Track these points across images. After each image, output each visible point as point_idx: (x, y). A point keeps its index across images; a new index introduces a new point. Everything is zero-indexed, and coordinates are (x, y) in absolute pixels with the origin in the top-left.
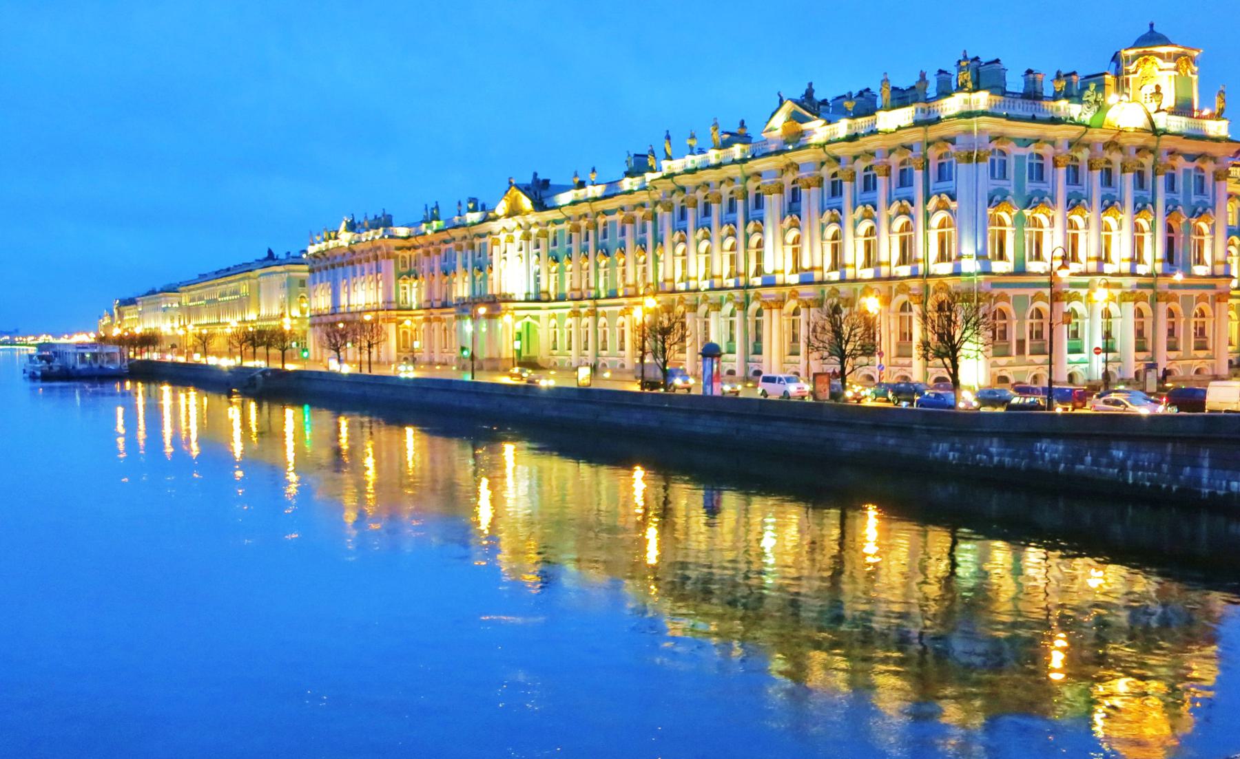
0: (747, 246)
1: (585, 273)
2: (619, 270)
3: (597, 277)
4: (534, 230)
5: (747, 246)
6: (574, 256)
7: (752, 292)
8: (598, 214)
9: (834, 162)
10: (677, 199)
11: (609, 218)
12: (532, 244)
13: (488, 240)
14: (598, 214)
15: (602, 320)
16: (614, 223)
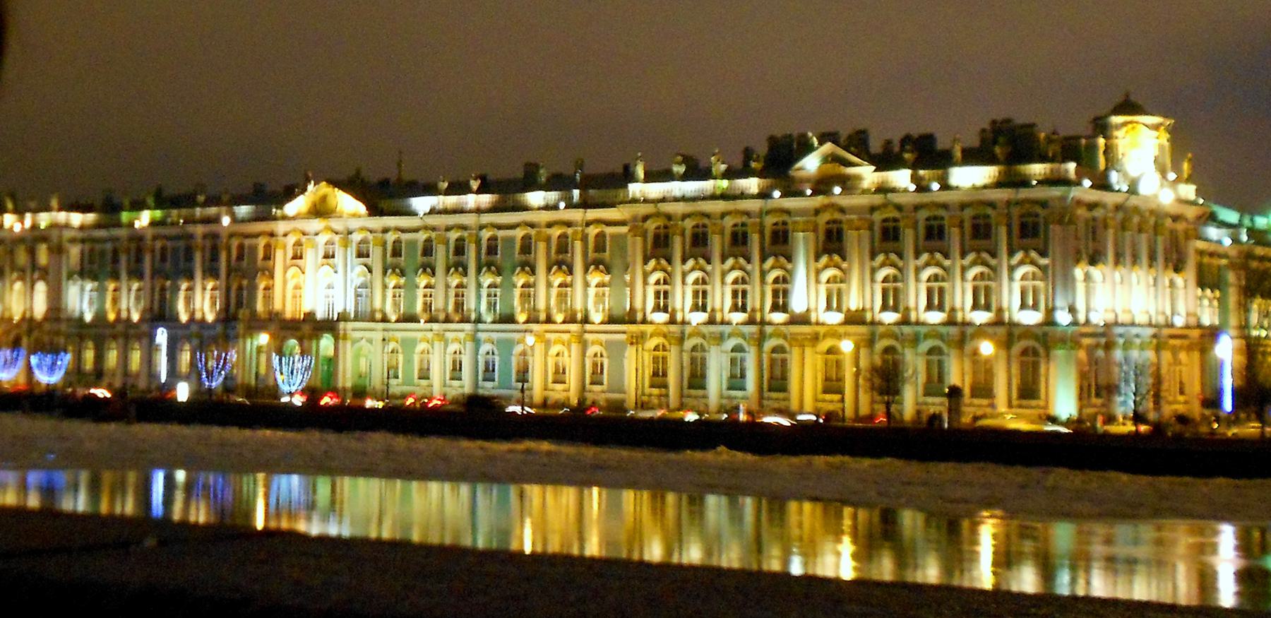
0: (763, 281)
1: (452, 293)
2: (517, 292)
3: (479, 297)
4: (357, 237)
5: (763, 281)
6: (440, 270)
7: (769, 329)
8: (481, 227)
9: (891, 208)
10: (651, 225)
11: (501, 233)
12: (352, 251)
13: (262, 242)
14: (481, 227)
15: (485, 348)
16: (511, 240)
